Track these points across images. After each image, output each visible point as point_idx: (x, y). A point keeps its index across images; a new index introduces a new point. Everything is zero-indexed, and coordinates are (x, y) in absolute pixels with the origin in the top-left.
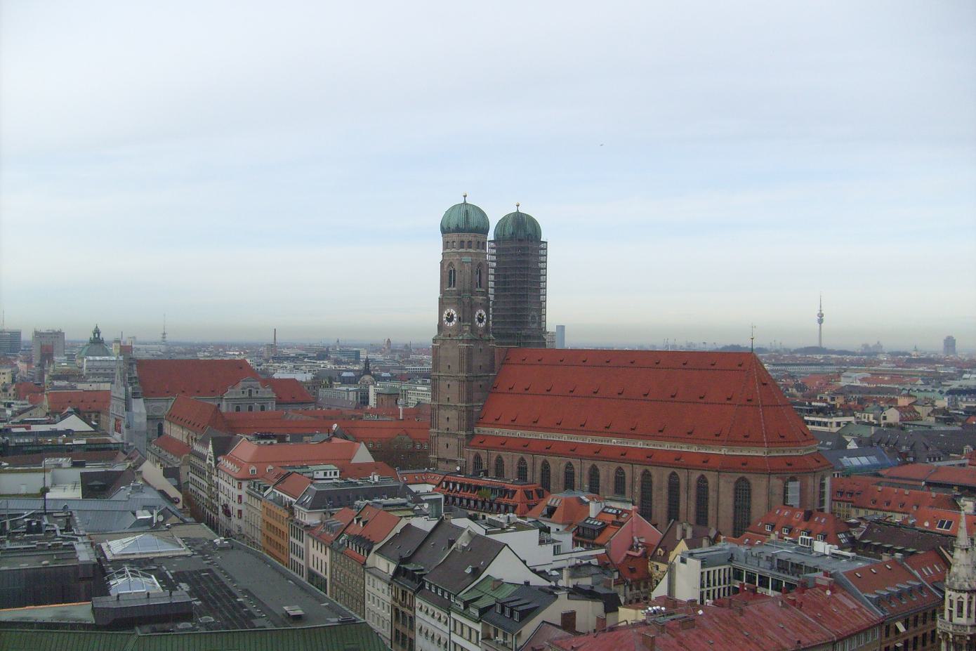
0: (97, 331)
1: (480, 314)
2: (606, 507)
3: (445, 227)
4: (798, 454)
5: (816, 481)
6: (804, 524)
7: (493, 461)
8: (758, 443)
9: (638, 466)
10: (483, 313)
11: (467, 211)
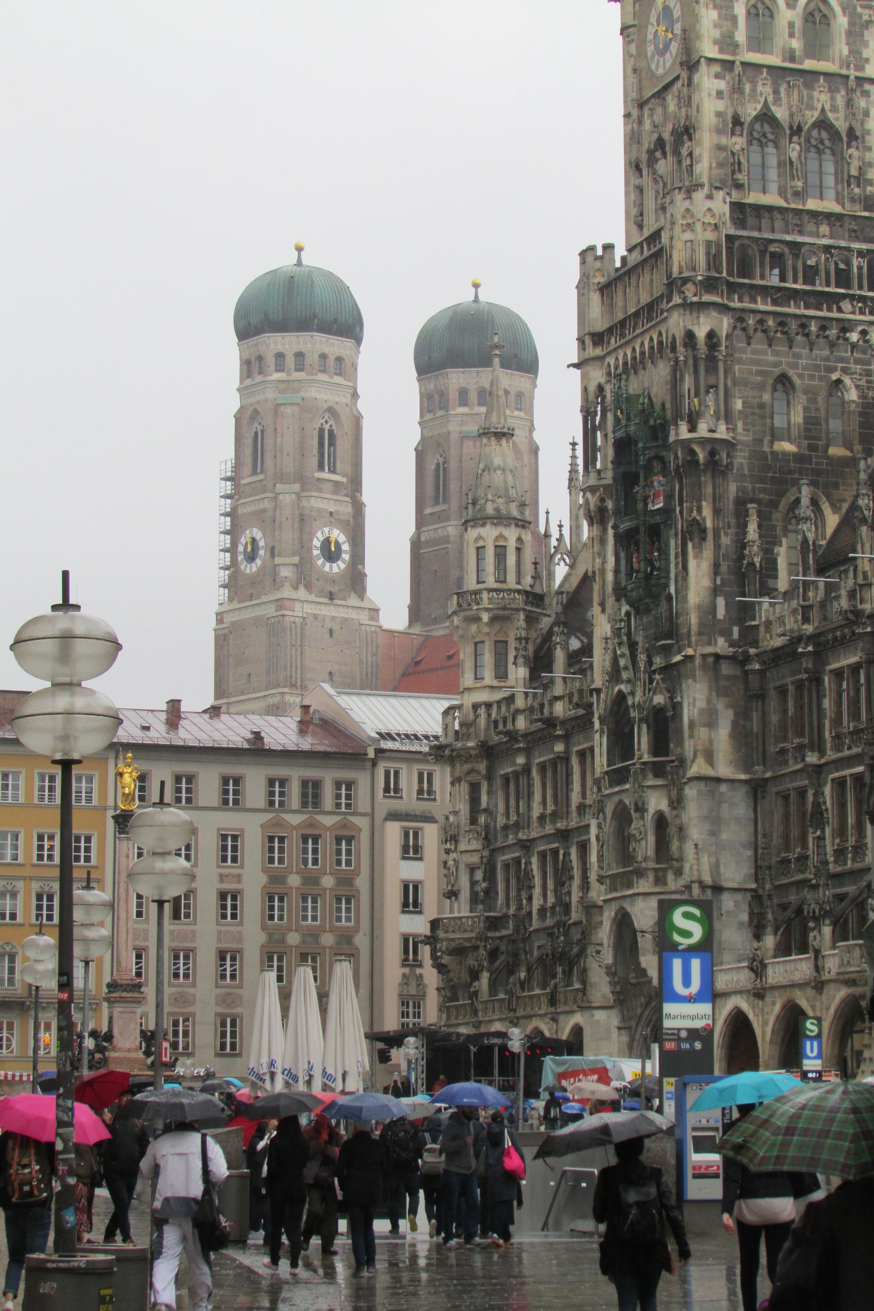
1: (327, 542)
10: (338, 535)
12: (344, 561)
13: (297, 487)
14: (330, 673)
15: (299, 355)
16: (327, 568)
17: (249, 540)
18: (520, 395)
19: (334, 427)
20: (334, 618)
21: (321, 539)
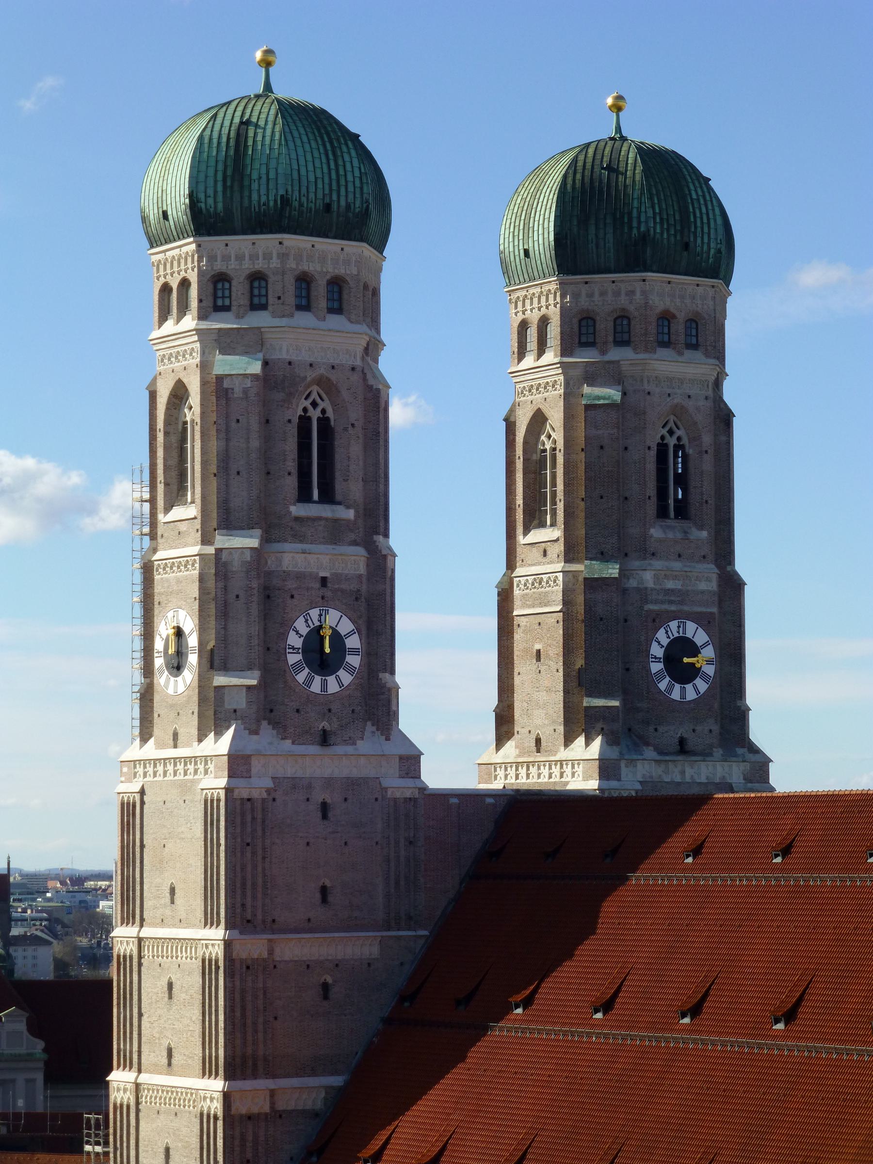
1: (315, 636)
3: (153, 214)
12: (350, 669)
14: (324, 891)
15: (257, 278)
16: (316, 687)
17: (171, 631)
18: (694, 322)
19: (330, 413)
20: (329, 782)
21: (304, 631)
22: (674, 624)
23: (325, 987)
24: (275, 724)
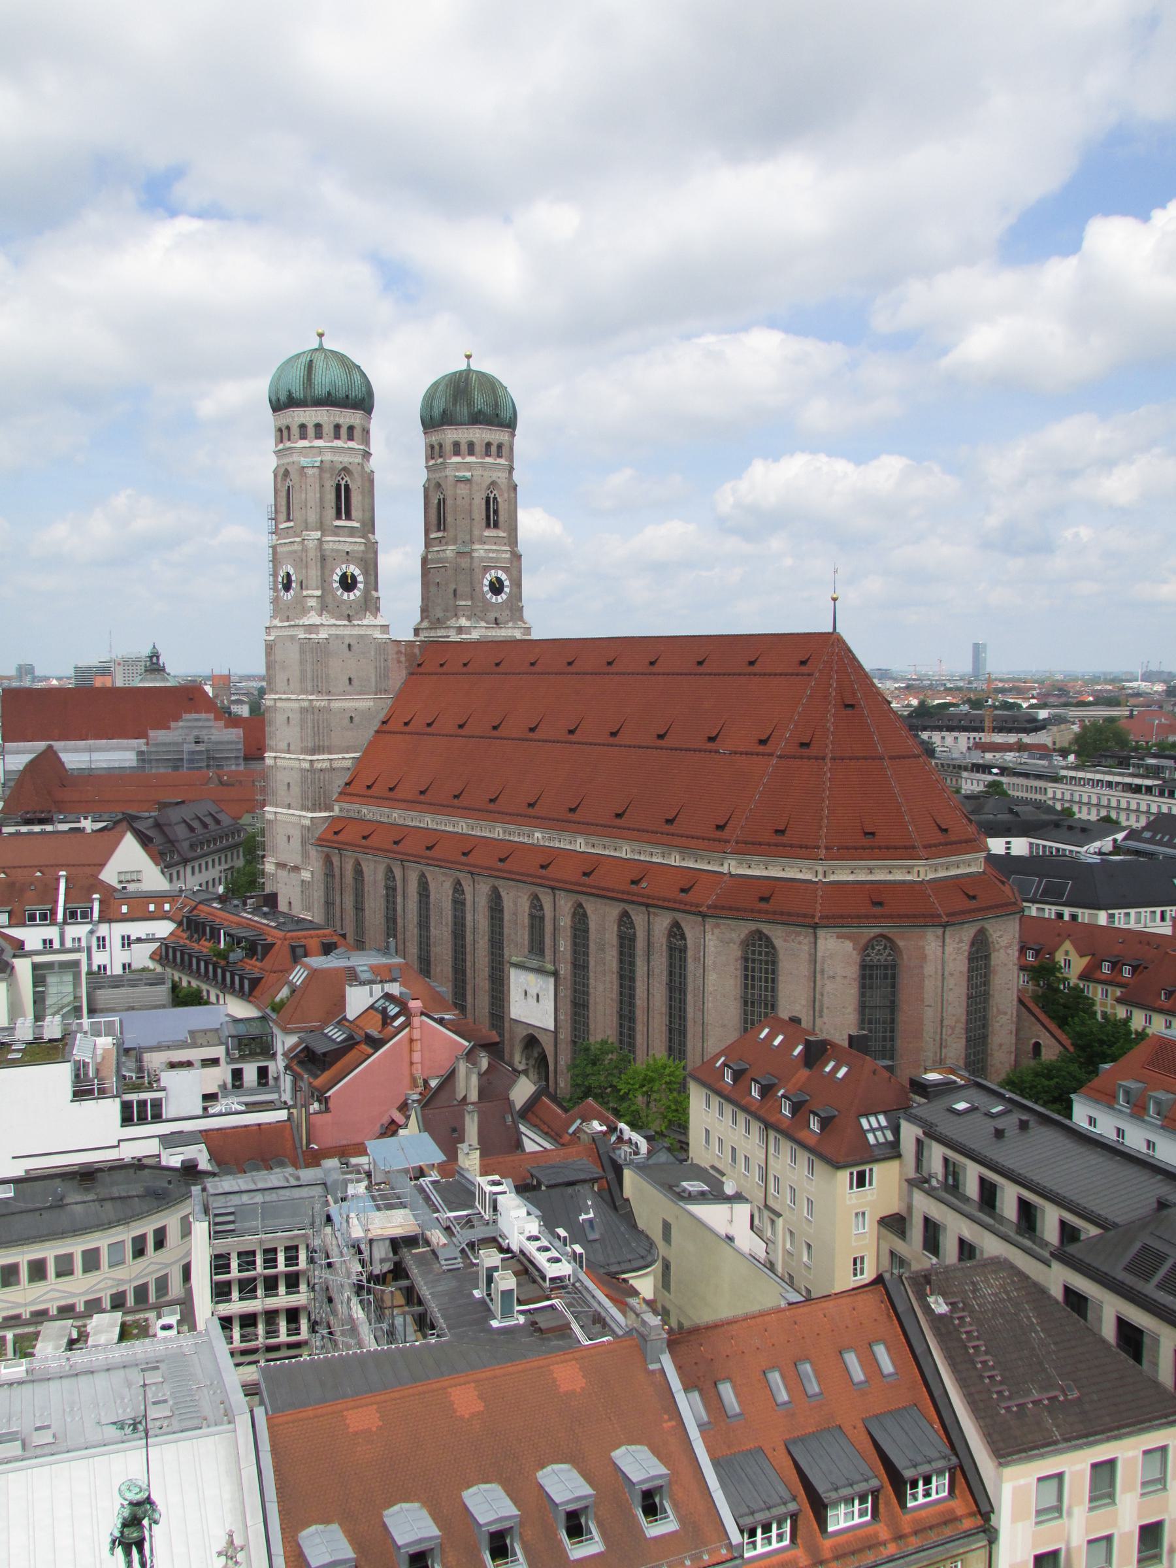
0: (155, 655)
1: (344, 577)
2: (388, 996)
3: (274, 399)
4: (909, 878)
5: (948, 949)
6: (804, 1073)
7: (349, 867)
8: (804, 850)
9: (563, 894)
11: (311, 361)
12: (359, 590)
13: (319, 533)
14: (350, 679)
15: (318, 426)
19: (349, 482)
21: (340, 574)
22: (493, 571)
23: (351, 718)
24: (328, 612)
